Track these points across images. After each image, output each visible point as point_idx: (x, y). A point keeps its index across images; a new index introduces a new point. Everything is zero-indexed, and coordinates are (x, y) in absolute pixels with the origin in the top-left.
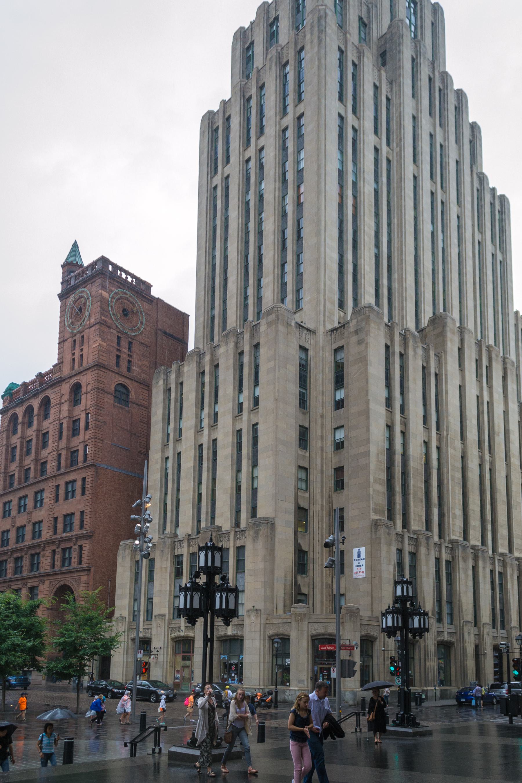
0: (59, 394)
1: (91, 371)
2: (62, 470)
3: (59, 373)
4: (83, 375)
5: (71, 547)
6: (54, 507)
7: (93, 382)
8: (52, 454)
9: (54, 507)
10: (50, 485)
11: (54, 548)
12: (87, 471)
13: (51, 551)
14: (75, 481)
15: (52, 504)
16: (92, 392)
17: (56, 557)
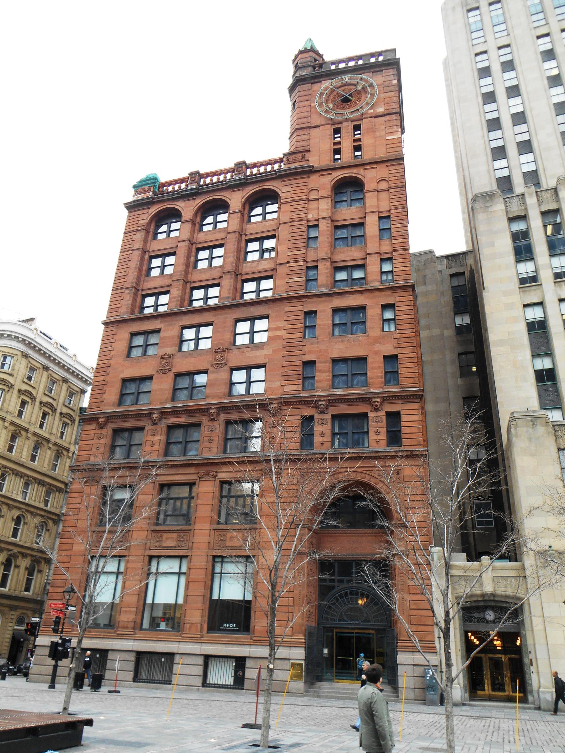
0: (305, 187)
1: (387, 166)
2: (324, 290)
3: (301, 164)
4: (364, 169)
5: (365, 415)
6: (301, 344)
7: (396, 178)
8: (288, 265)
9: (301, 344)
10: (287, 309)
11: (308, 412)
12: (397, 294)
13: (299, 417)
14: (362, 309)
15: (300, 340)
16: (391, 191)
17: (318, 429)
